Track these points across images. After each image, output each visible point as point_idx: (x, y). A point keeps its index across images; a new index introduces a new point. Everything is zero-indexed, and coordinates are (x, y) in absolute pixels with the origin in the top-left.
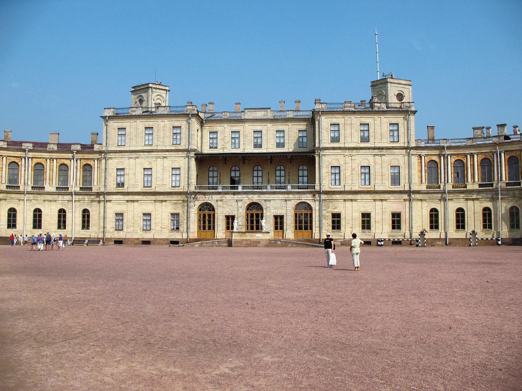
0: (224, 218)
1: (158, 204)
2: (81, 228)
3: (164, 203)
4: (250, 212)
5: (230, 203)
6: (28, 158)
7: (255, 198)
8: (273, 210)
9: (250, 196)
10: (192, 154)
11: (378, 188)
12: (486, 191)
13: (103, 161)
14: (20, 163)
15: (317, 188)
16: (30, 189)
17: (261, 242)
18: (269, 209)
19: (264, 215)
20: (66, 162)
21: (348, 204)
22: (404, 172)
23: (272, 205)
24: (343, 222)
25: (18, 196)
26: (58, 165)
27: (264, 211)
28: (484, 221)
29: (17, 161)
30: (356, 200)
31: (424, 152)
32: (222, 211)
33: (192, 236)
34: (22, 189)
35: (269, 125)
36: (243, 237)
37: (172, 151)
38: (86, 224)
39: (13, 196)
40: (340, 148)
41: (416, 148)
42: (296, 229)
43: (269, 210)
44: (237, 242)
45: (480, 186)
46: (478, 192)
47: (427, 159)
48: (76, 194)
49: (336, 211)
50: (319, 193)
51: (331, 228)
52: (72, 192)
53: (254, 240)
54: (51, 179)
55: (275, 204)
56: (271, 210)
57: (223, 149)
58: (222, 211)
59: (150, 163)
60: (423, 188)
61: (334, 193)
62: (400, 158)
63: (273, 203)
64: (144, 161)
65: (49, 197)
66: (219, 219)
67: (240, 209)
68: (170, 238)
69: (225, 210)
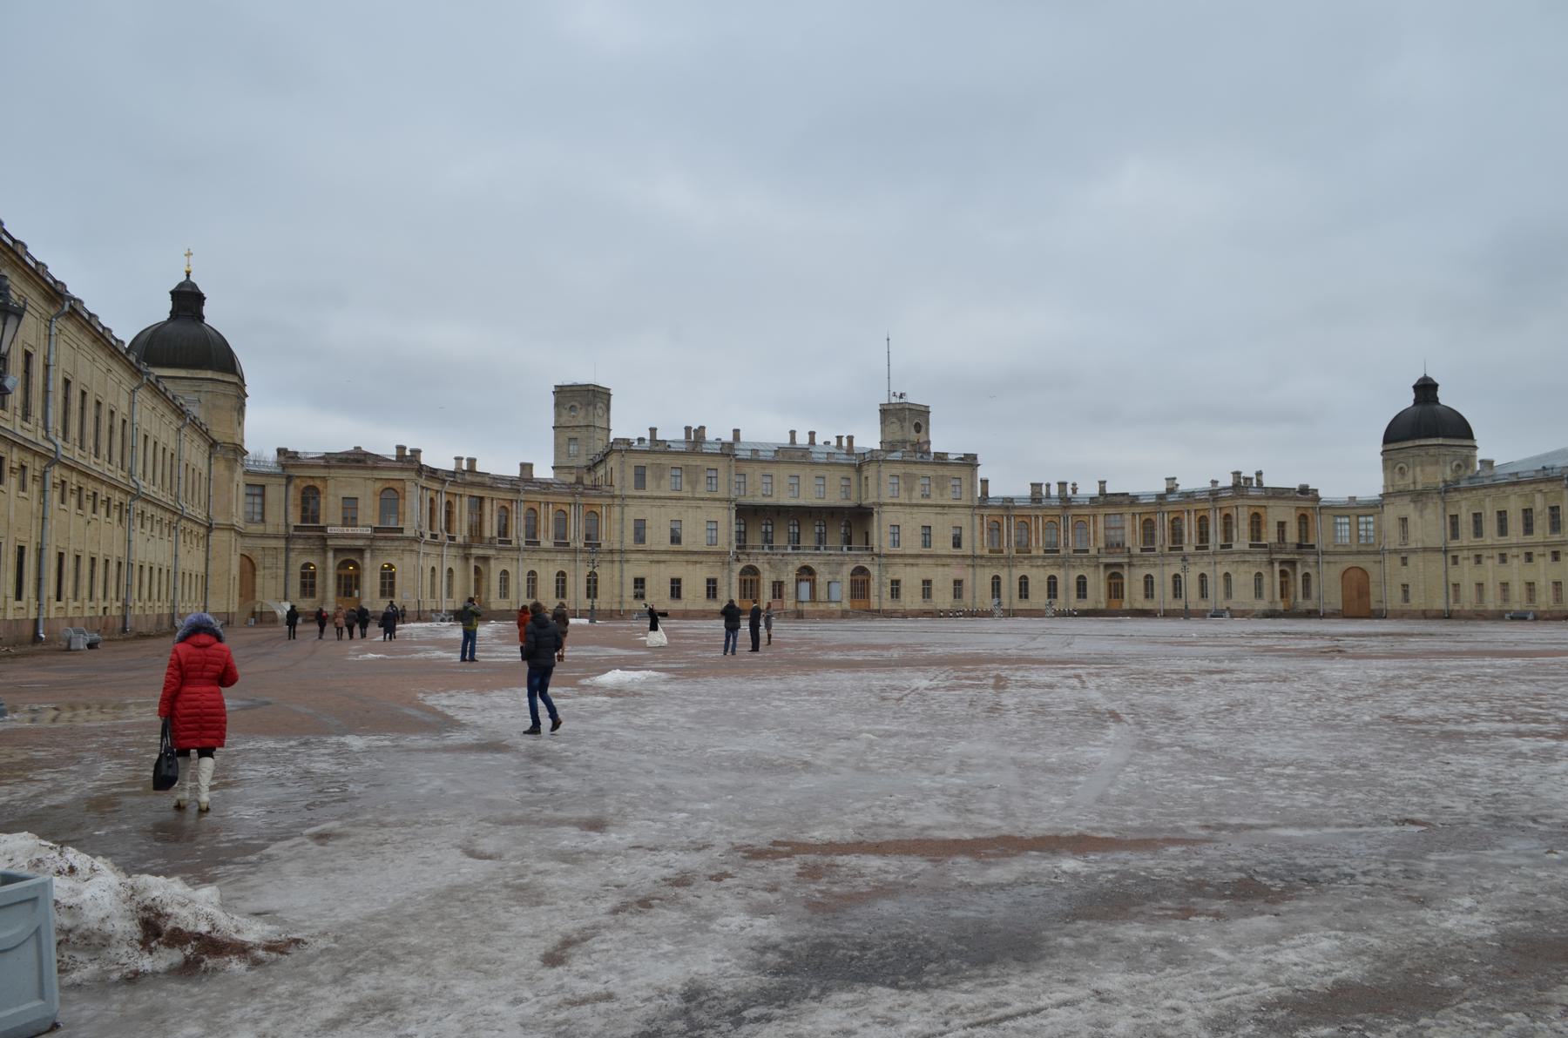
1: (690, 567)
3: (698, 566)
4: (800, 577)
7: (807, 561)
9: (802, 557)
10: (733, 505)
11: (939, 552)
12: (1052, 557)
13: (617, 509)
15: (876, 550)
19: (817, 581)
20: (566, 508)
21: (908, 569)
22: (966, 535)
24: (902, 591)
25: (510, 553)
27: (818, 576)
28: (1049, 590)
30: (917, 565)
31: (986, 512)
34: (514, 542)
35: (808, 469)
37: (708, 499)
38: (592, 591)
39: (506, 553)
40: (900, 505)
41: (980, 507)
42: (852, 597)
44: (809, 612)
45: (1046, 551)
46: (1044, 558)
47: (991, 519)
48: (581, 551)
49: (896, 577)
50: (876, 555)
51: (889, 596)
54: (547, 531)
57: (753, 496)
59: (680, 514)
60: (986, 552)
61: (894, 556)
62: (963, 519)
64: (672, 512)
65: (546, 556)
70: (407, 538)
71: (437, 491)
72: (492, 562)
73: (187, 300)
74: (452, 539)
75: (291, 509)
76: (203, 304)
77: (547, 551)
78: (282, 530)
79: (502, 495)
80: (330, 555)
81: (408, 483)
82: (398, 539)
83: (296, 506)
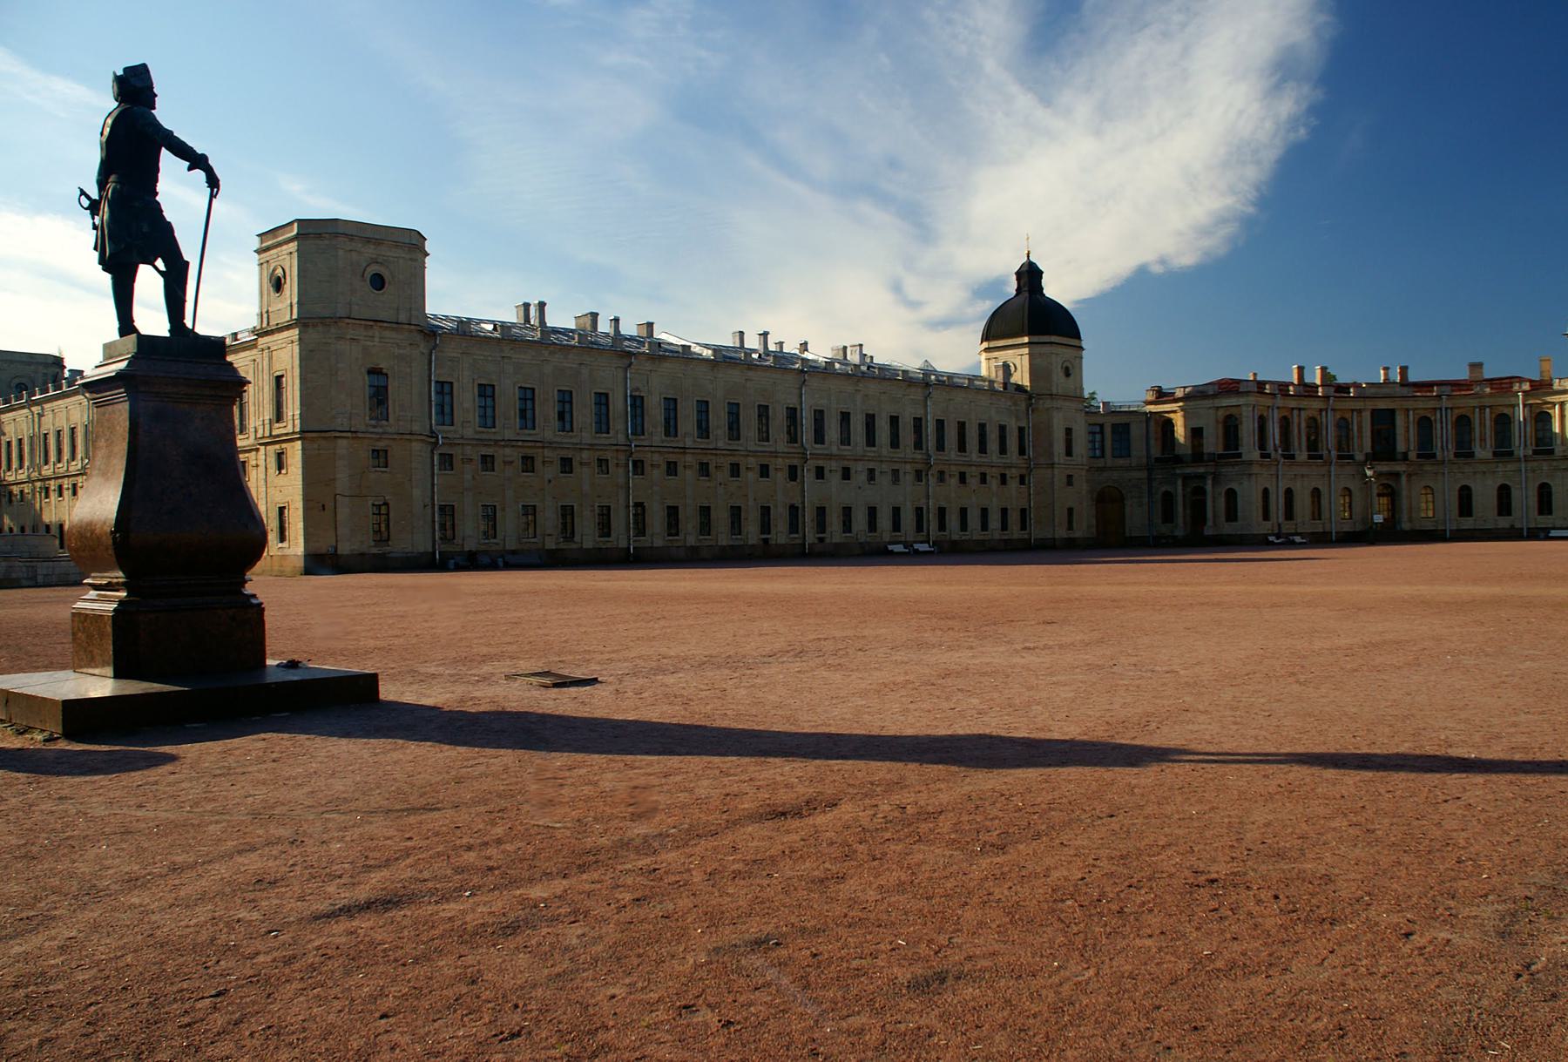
2: (1536, 512)
6: (1446, 409)
14: (1433, 418)
16: (1452, 456)
26: (1494, 416)
29: (1429, 415)
34: (1439, 454)
39: (1428, 468)
52: (1525, 461)
54: (1483, 439)
70: (1243, 462)
71: (1321, 410)
72: (1404, 479)
73: (1030, 276)
74: (1292, 457)
75: (1152, 442)
76: (1041, 278)
77: (1483, 462)
78: (1144, 460)
79: (1420, 405)
80: (1180, 482)
81: (1244, 408)
82: (1236, 464)
83: (1156, 439)
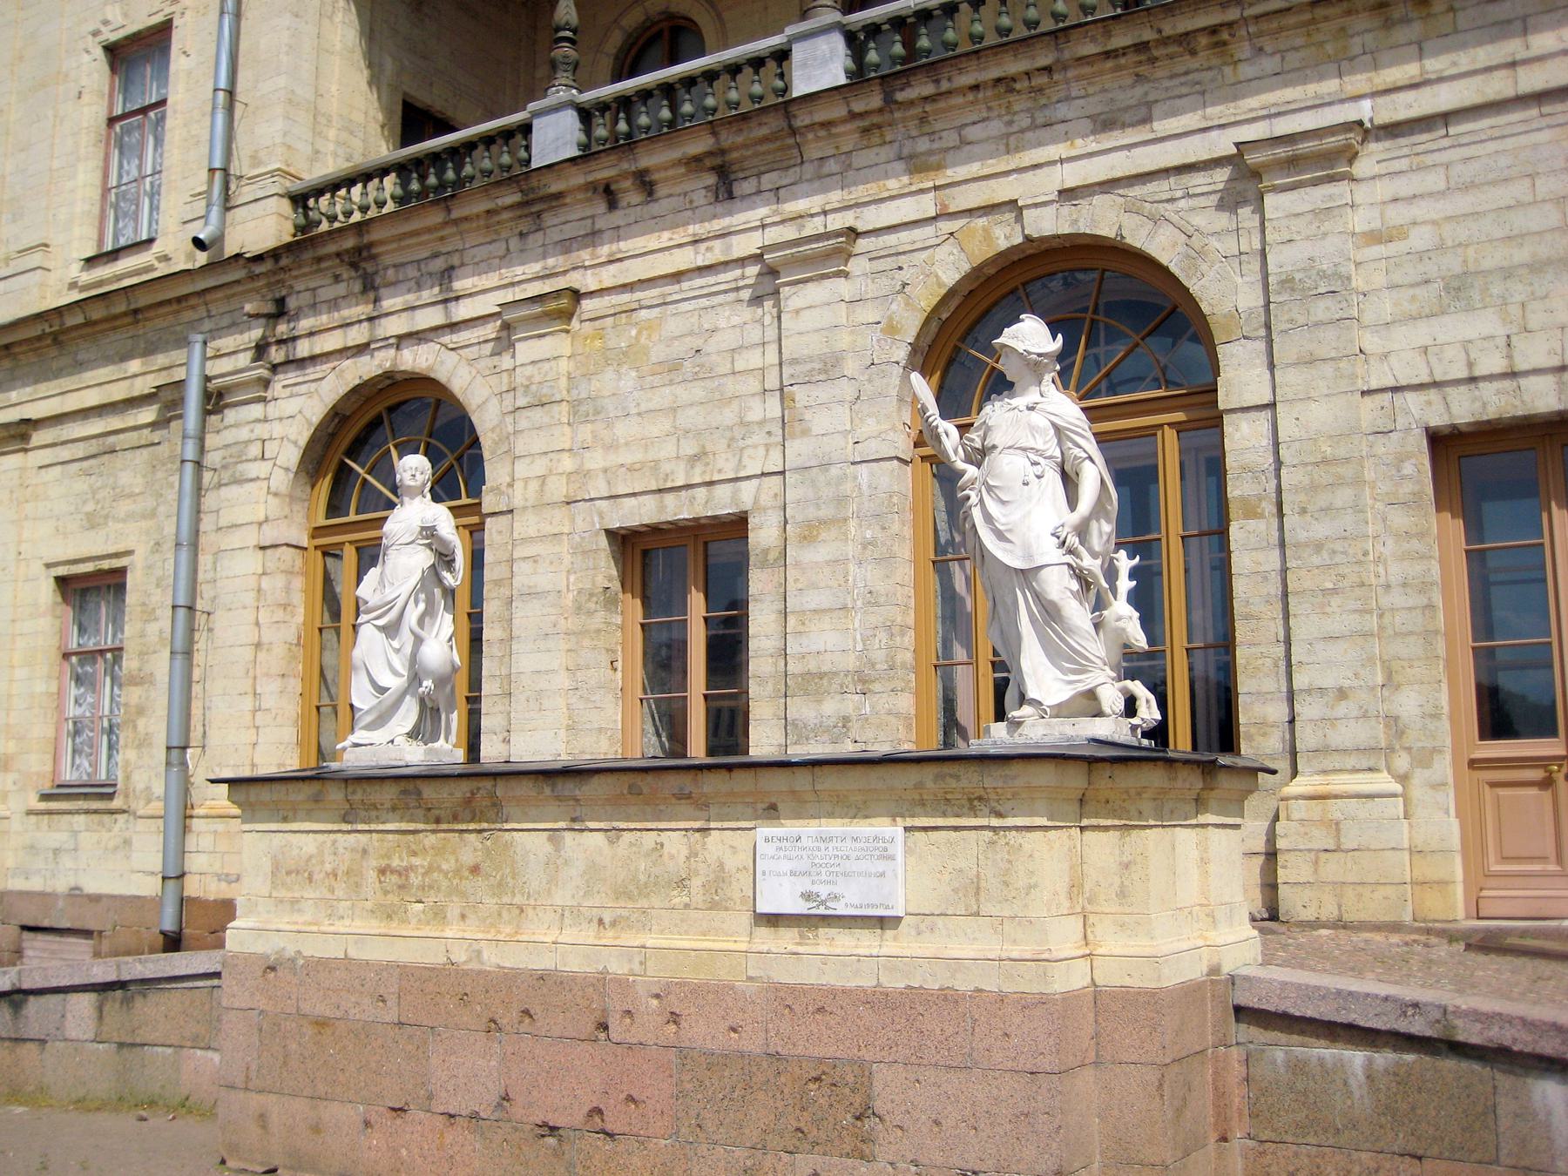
0: (605, 570)
5: (673, 326)
8: (1421, 333)
17: (889, 1087)
18: (1322, 309)
23: (1375, 237)
32: (567, 463)
33: (217, 867)
36: (439, 915)
43: (1327, 343)
53: (703, 1032)
55: (1420, 211)
56: (1371, 342)
58: (567, 463)
63: (1403, 186)
66: (532, 594)
67: (822, 393)
68: (36, 884)
69: (612, 447)
